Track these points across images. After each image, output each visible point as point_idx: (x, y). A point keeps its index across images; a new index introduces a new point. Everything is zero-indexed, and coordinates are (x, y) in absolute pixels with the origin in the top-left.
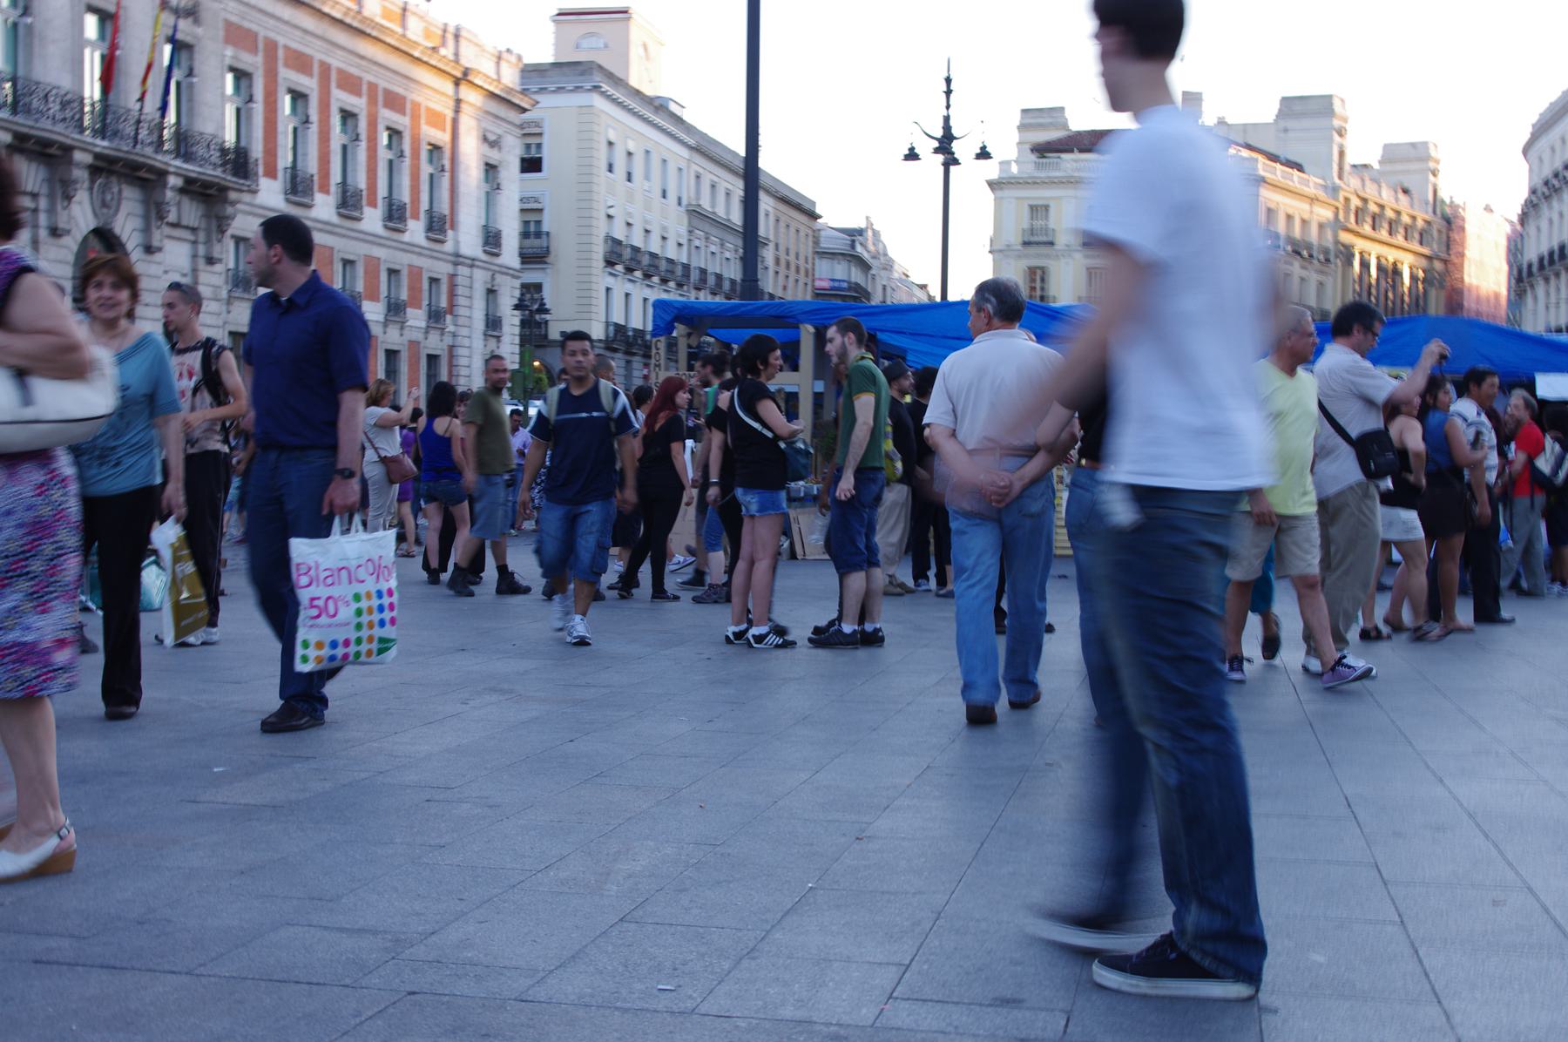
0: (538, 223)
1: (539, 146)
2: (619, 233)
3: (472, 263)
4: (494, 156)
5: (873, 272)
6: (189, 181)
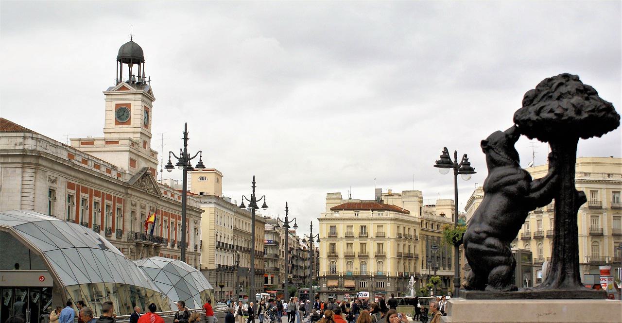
3: (192, 254)
4: (196, 226)
5: (280, 236)
6: (145, 245)
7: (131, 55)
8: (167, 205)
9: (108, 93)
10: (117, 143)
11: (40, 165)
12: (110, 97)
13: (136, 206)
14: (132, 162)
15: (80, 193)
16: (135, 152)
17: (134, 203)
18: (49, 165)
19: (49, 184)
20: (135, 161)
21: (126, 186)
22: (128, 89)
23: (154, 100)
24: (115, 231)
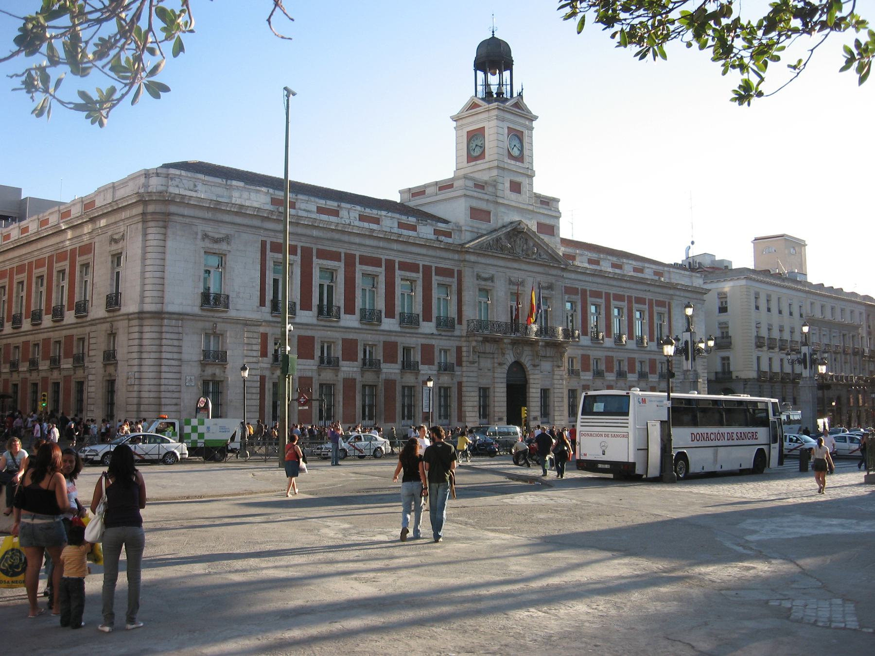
0: (727, 332)
1: (726, 302)
2: (764, 333)
7: (494, 57)
8: (600, 280)
9: (456, 119)
10: (451, 186)
11: (169, 214)
12: (460, 122)
13: (493, 281)
14: (476, 213)
15: (314, 258)
16: (491, 198)
18: (209, 215)
19: (208, 244)
20: (488, 213)
21: (461, 249)
22: (479, 106)
23: (536, 118)
24: (434, 319)
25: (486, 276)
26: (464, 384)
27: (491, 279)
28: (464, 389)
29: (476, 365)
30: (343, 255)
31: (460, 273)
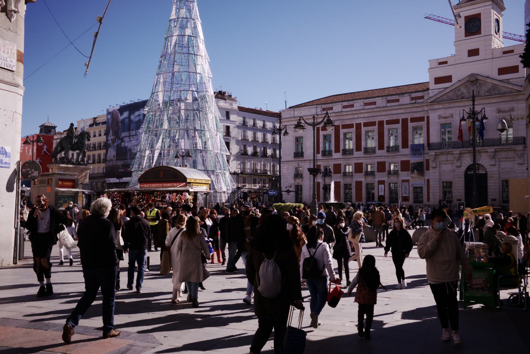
13: (452, 117)
17: (444, 115)
25: (447, 115)
26: (430, 180)
27: (452, 116)
28: (430, 183)
29: (438, 169)
30: (355, 125)
31: (428, 117)
